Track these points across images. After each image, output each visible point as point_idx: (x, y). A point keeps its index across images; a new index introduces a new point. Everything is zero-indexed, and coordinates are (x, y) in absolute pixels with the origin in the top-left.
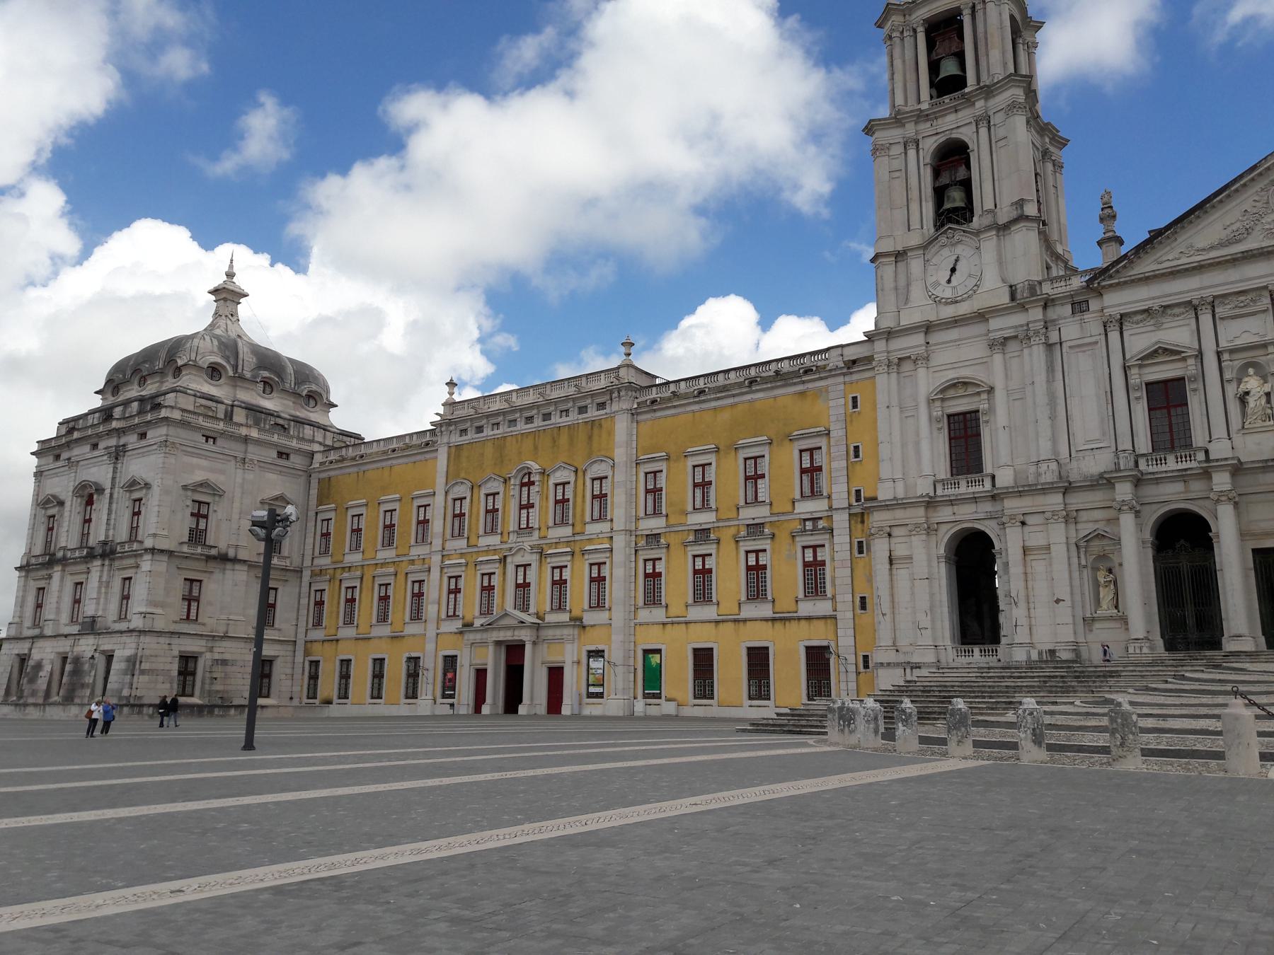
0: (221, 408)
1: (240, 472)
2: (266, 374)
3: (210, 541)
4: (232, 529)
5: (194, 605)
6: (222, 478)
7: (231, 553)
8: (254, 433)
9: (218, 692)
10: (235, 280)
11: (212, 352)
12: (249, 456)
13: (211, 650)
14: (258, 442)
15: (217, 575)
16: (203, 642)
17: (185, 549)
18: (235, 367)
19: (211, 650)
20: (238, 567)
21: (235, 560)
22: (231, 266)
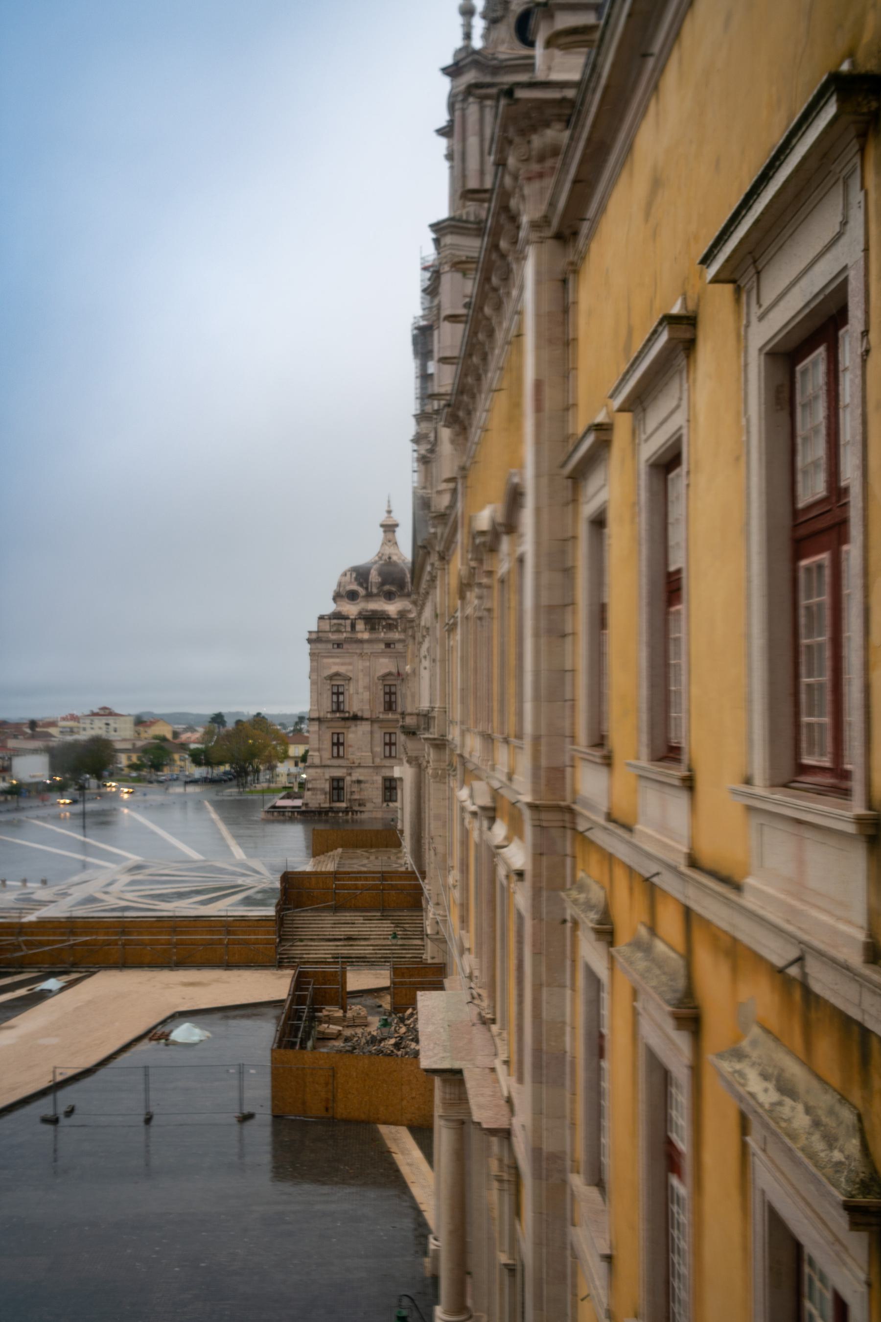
0: (348, 622)
1: (360, 662)
2: (387, 588)
3: (347, 709)
4: (360, 698)
5: (341, 748)
6: (350, 668)
7: (359, 714)
8: (366, 636)
9: (355, 800)
10: (392, 515)
11: (351, 582)
12: (365, 651)
13: (350, 774)
14: (369, 641)
15: (353, 729)
16: (345, 770)
17: (329, 716)
18: (367, 589)
19: (350, 774)
20: (364, 723)
21: (362, 719)
22: (389, 506)
